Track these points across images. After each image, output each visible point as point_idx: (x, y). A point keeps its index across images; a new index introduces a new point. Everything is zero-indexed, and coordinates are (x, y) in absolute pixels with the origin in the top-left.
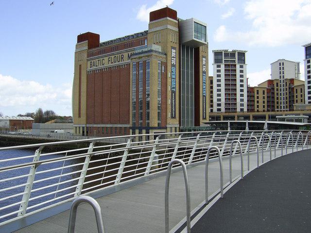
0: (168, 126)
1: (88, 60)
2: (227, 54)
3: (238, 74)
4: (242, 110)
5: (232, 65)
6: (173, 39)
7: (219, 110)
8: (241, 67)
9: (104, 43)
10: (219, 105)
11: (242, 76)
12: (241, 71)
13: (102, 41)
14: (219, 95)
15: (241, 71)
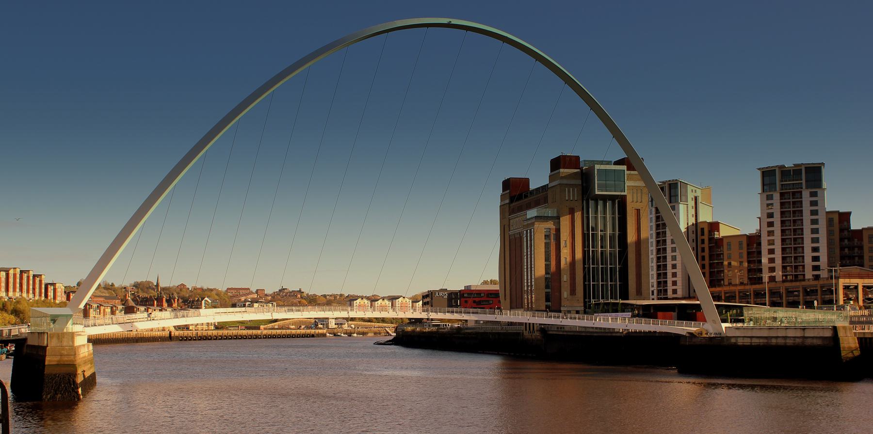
0: (562, 309)
2: (785, 173)
3: (806, 208)
4: (817, 277)
5: (794, 193)
6: (573, 195)
7: (772, 279)
8: (814, 194)
9: (537, 189)
10: (816, 268)
11: (814, 213)
12: (814, 203)
13: (533, 186)
14: (771, 251)
15: (814, 203)
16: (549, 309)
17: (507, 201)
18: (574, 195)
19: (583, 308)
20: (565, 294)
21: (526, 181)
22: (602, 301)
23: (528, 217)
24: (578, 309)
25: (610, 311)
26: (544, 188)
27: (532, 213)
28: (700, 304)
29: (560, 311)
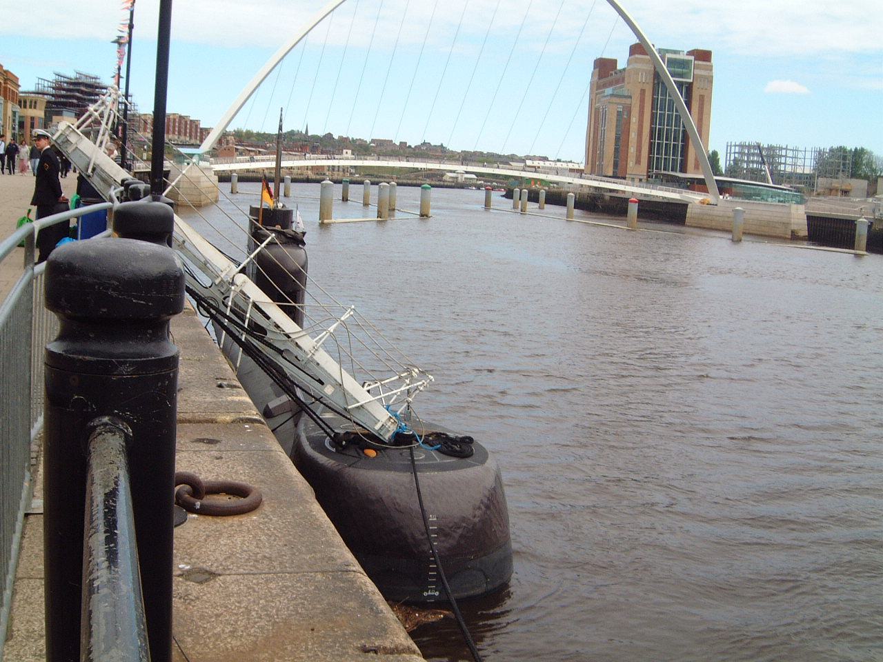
0: (627, 176)
1: (597, 94)
16: (615, 176)
17: (596, 78)
18: (646, 79)
19: (645, 177)
20: (631, 164)
21: (614, 62)
22: (663, 172)
23: (606, 94)
24: (641, 177)
25: (326, 169)
26: (624, 69)
27: (609, 91)
28: (703, 179)
29: (625, 178)
